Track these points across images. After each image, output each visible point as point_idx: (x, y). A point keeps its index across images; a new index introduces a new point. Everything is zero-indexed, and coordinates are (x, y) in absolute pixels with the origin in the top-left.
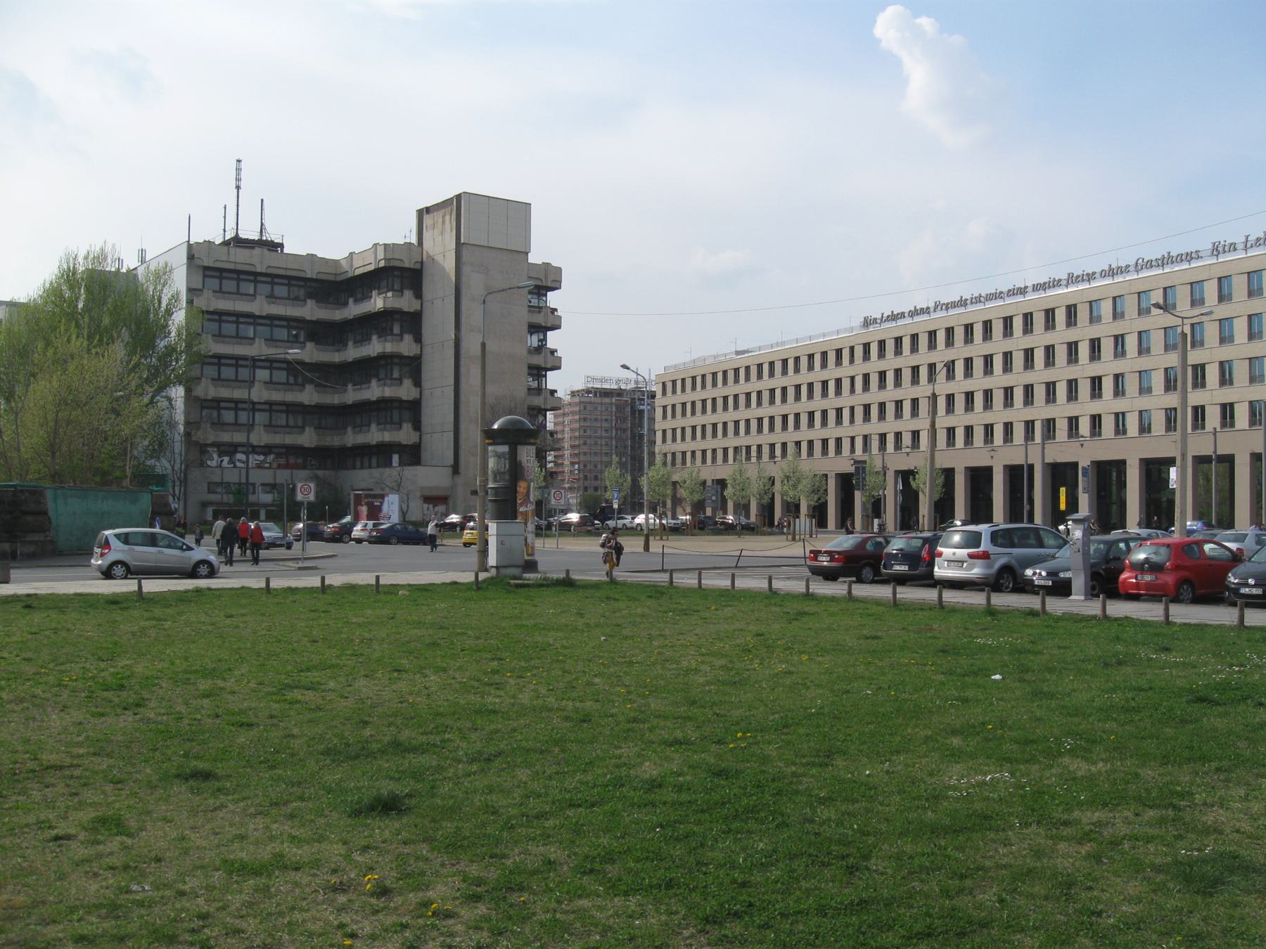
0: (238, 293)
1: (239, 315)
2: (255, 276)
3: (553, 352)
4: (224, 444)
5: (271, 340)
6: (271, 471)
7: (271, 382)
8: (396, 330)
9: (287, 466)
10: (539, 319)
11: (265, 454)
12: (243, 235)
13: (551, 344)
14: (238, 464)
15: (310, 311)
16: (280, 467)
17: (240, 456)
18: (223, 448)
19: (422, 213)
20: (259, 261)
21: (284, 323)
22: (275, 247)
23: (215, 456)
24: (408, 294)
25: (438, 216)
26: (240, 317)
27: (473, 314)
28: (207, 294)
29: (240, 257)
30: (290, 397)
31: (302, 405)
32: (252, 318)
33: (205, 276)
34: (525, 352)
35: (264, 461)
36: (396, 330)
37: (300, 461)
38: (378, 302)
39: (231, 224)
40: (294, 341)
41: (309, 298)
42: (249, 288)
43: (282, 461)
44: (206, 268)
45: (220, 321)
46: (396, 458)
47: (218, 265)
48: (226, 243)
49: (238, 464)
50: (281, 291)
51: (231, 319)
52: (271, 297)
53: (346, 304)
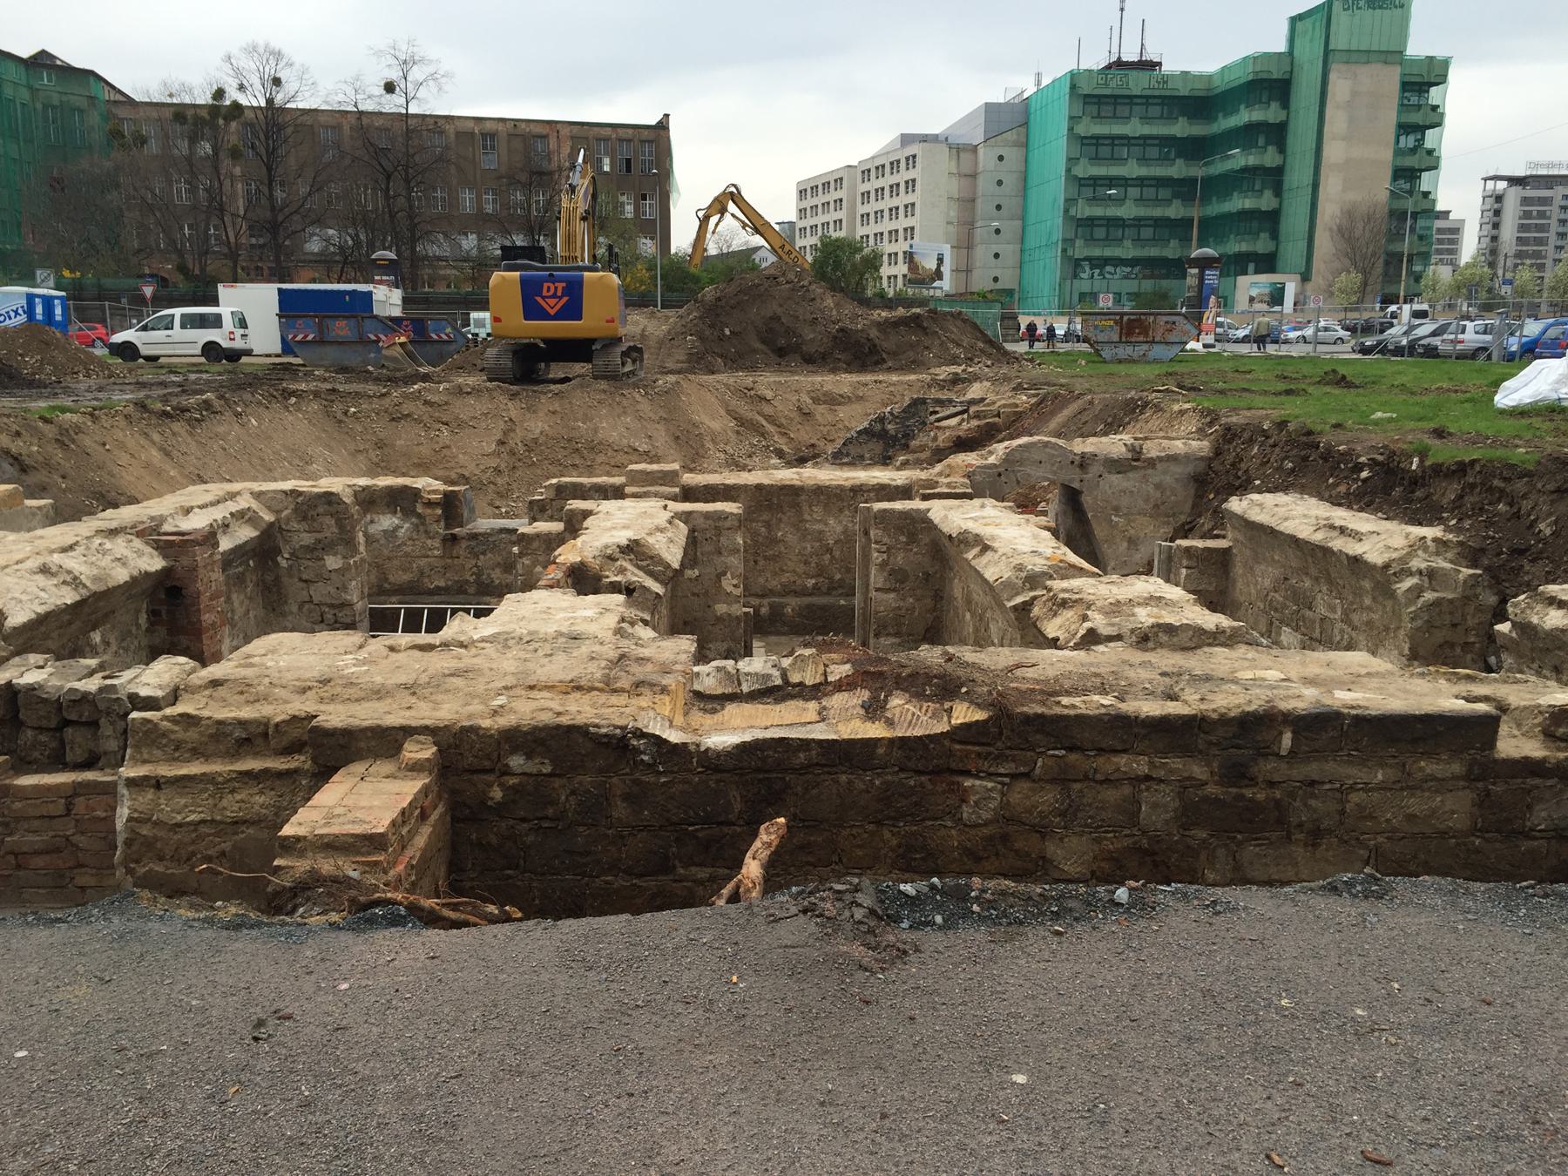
0: (1115, 117)
1: (1113, 138)
2: (1130, 100)
3: (1430, 152)
4: (1098, 258)
5: (1143, 160)
6: (1136, 282)
7: (1141, 199)
8: (1261, 141)
9: (1151, 277)
10: (1415, 118)
11: (1132, 267)
12: (1124, 59)
13: (1428, 144)
14: (1107, 276)
15: (1180, 128)
16: (1145, 277)
17: (1109, 268)
18: (1094, 262)
19: (1295, 20)
20: (1138, 84)
21: (1157, 142)
22: (1153, 65)
23: (1087, 269)
24: (1274, 105)
25: (1308, 23)
26: (1114, 140)
27: (1336, 120)
28: (1086, 120)
29: (1115, 85)
30: (1158, 212)
31: (1168, 219)
32: (1126, 140)
33: (1085, 103)
34: (1387, 155)
35: (1131, 272)
36: (1261, 141)
37: (1164, 271)
38: (1245, 116)
39: (1115, 49)
40: (1164, 159)
41: (1183, 115)
42: (1123, 110)
43: (1147, 272)
44: (1086, 96)
45: (1097, 145)
46: (1251, 267)
47: (1097, 92)
48: (1109, 67)
49: (1107, 276)
50: (1155, 111)
51: (1106, 142)
52: (1145, 119)
53: (1216, 119)
